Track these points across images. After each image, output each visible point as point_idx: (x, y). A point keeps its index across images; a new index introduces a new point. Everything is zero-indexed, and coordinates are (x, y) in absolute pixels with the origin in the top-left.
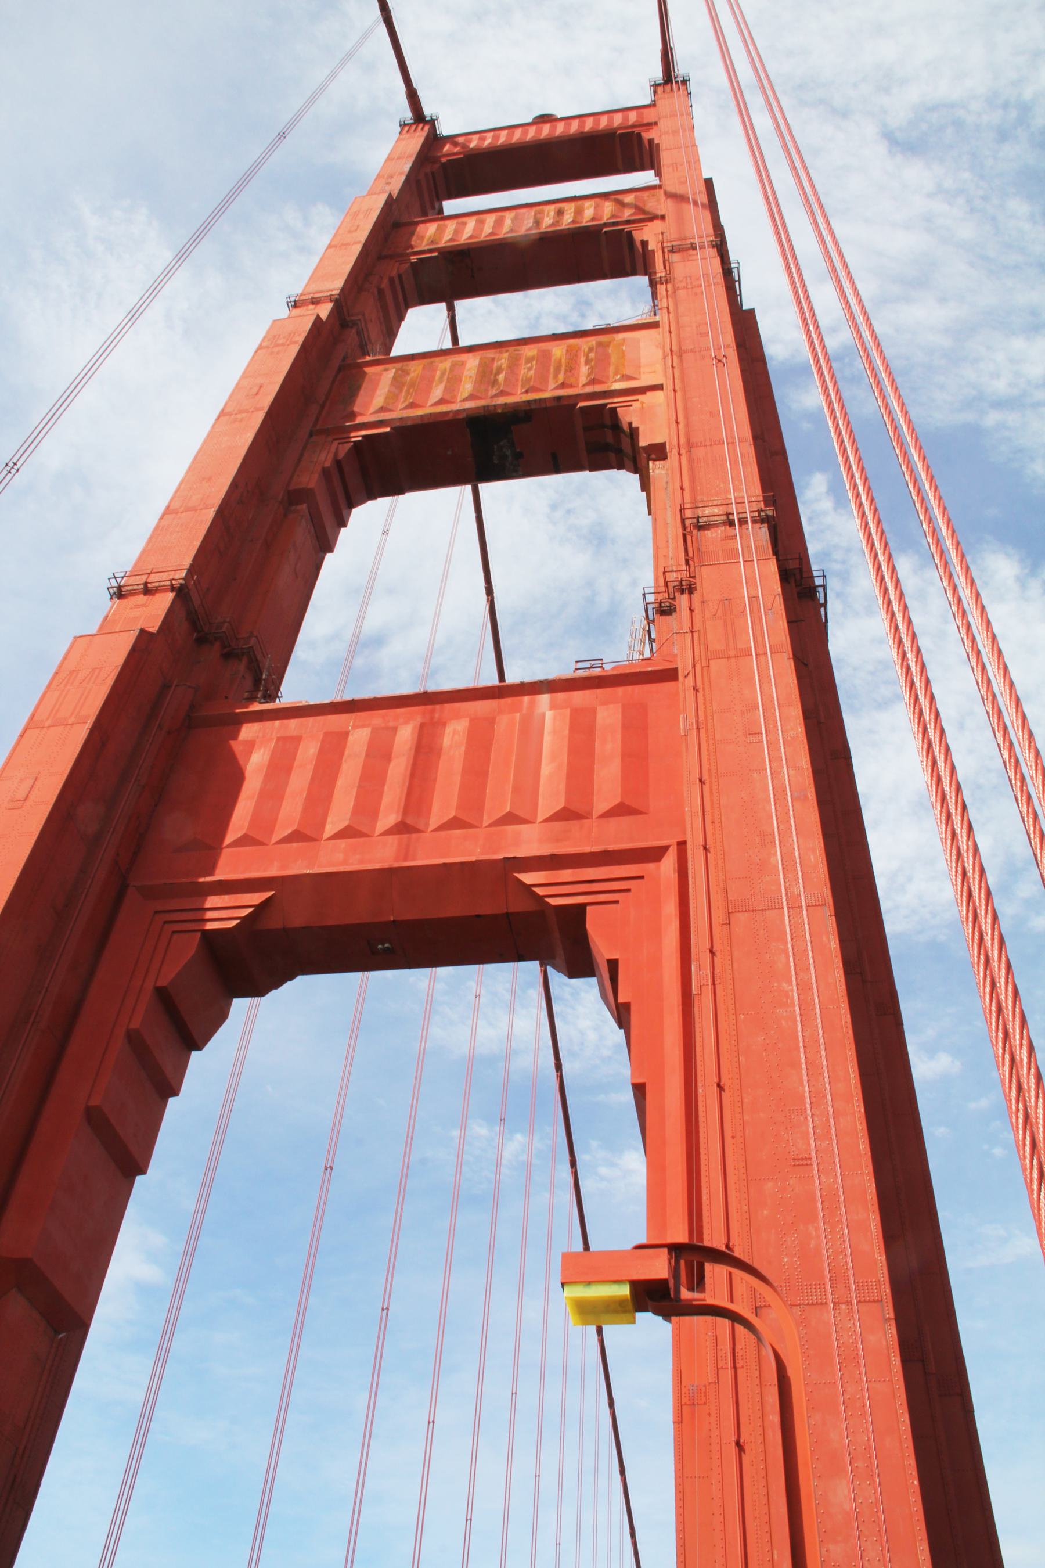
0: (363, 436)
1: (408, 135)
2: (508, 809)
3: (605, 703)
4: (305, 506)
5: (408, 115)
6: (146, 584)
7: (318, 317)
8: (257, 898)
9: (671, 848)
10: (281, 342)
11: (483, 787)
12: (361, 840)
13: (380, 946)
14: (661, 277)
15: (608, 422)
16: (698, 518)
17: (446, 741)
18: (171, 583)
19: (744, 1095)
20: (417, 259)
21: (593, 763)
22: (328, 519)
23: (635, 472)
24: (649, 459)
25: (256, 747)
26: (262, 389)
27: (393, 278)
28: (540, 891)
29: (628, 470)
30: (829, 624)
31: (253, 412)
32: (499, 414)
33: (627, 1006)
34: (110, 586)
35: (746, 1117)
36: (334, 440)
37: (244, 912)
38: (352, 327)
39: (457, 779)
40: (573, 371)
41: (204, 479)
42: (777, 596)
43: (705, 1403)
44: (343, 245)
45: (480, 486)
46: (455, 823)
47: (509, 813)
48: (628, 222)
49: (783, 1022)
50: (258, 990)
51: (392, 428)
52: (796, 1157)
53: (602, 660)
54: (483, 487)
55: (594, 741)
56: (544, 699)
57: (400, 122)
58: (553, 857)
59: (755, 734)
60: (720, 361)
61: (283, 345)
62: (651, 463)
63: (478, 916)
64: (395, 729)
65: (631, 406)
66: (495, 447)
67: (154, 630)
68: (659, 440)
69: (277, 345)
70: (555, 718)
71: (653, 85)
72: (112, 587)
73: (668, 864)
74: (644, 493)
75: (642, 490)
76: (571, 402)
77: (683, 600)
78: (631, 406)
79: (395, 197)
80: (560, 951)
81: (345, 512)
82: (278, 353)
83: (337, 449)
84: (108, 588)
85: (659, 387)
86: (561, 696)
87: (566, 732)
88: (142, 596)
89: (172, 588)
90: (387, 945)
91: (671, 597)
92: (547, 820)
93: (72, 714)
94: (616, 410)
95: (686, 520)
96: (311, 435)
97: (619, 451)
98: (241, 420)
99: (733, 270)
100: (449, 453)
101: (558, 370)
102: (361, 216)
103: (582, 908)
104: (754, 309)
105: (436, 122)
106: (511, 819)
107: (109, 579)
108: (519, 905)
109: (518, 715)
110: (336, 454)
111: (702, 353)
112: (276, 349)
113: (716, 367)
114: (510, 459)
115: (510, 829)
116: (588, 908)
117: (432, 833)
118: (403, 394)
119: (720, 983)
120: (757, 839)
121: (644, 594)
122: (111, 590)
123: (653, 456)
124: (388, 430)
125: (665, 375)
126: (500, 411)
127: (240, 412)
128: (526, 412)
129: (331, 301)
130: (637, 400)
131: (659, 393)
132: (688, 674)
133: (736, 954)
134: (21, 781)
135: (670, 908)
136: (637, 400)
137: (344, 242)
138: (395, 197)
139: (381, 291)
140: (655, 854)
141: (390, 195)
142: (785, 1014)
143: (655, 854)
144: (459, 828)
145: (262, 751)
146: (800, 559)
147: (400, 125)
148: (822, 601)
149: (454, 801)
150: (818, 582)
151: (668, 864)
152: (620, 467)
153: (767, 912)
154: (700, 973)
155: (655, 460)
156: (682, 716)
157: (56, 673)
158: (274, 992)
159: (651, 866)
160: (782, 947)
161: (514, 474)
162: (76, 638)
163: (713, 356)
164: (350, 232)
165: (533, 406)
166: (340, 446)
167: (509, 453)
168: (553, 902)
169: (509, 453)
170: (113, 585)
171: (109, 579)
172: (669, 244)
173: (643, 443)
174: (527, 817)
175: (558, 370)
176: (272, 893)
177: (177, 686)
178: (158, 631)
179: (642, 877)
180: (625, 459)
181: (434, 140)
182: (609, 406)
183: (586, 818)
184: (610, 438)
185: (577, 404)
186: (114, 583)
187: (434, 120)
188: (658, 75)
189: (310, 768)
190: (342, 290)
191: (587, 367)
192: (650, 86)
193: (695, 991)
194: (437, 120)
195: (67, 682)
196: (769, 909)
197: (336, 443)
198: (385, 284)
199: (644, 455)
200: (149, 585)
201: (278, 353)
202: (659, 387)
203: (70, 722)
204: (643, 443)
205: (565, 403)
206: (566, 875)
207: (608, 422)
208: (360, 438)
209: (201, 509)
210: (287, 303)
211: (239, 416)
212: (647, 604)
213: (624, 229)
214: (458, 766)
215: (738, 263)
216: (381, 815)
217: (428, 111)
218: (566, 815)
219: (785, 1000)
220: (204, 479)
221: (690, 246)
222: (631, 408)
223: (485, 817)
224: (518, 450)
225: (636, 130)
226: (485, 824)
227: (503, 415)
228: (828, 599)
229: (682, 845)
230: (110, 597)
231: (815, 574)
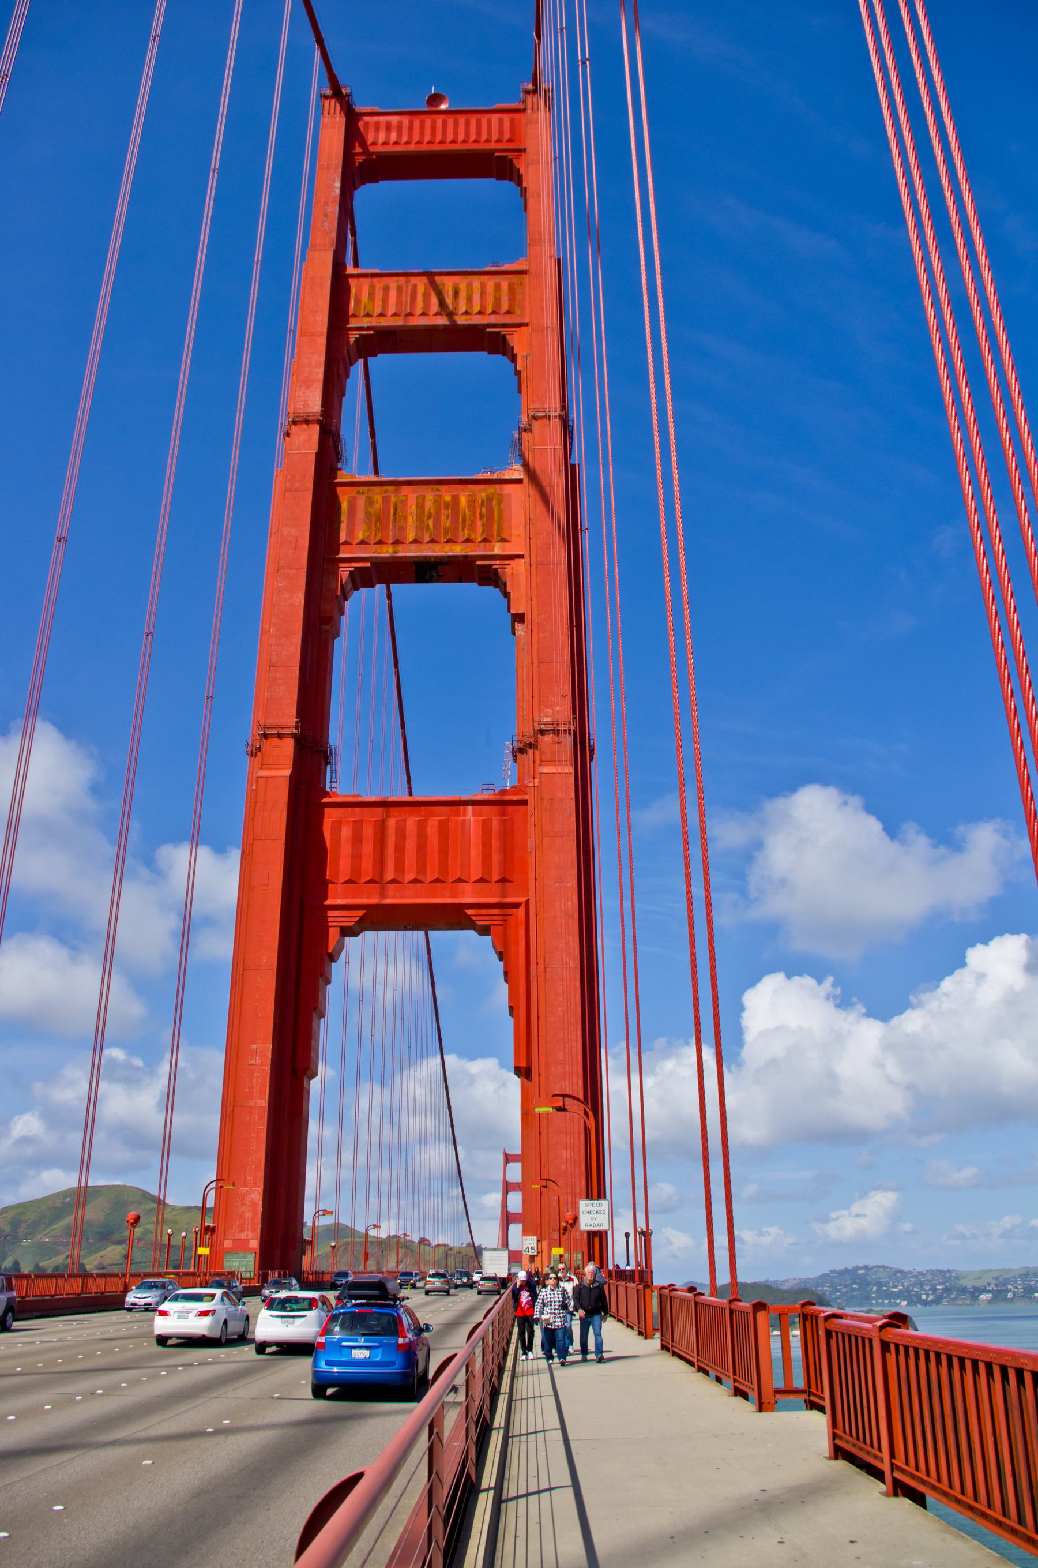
12: (400, 885)
20: (361, 335)
28: (473, 918)
29: (514, 183)
46: (437, 881)
68: (521, 611)
73: (521, 911)
85: (521, 557)
88: (276, 739)
106: (460, 880)
115: (460, 885)
123: (517, 620)
126: (433, 560)
135: (522, 932)
140: (517, 905)
151: (521, 911)
155: (518, 622)
159: (515, 910)
174: (467, 880)
185: (476, 561)
202: (521, 557)
206: (483, 911)
213: (500, 332)
214: (436, 847)
226: (450, 881)
229: (527, 901)
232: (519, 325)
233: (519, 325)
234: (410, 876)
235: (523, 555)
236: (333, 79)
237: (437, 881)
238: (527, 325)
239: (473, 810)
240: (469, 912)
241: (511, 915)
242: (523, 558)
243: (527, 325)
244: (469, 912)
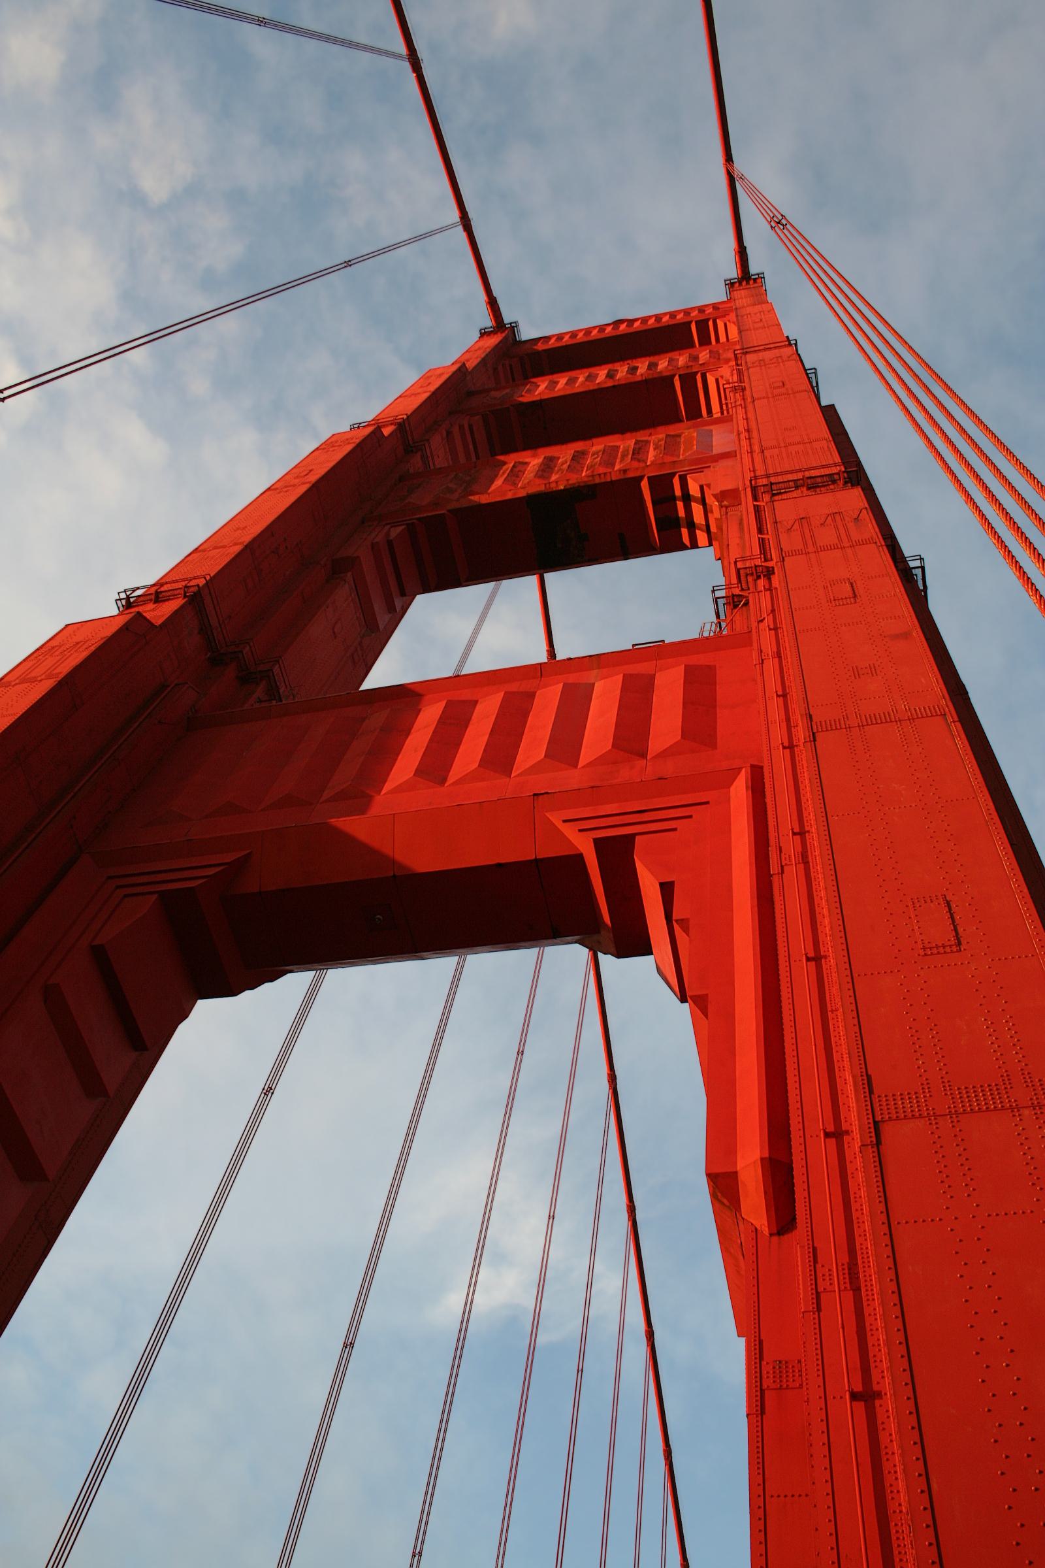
4: (349, 574)
6: (157, 593)
22: (378, 606)
26: (312, 473)
30: (929, 592)
32: (561, 490)
34: (118, 598)
36: (387, 524)
37: (211, 872)
42: (864, 511)
43: (801, 1386)
44: (413, 394)
45: (545, 575)
52: (927, 946)
54: (548, 577)
57: (480, 330)
61: (339, 446)
71: (728, 284)
72: (120, 599)
73: (740, 789)
83: (389, 530)
101: (624, 456)
102: (433, 378)
103: (630, 838)
105: (515, 328)
107: (119, 593)
110: (388, 534)
116: (637, 837)
121: (713, 591)
122: (119, 602)
127: (286, 487)
139: (449, 433)
146: (891, 535)
157: (38, 649)
158: (247, 994)
162: (67, 626)
164: (421, 387)
166: (393, 528)
170: (121, 598)
171: (119, 593)
175: (624, 456)
177: (176, 685)
179: (708, 803)
186: (123, 596)
187: (514, 327)
188: (733, 272)
192: (726, 285)
193: (774, 868)
194: (516, 327)
197: (388, 526)
199: (717, 503)
201: (334, 450)
211: (286, 489)
212: (716, 599)
217: (507, 318)
228: (928, 584)
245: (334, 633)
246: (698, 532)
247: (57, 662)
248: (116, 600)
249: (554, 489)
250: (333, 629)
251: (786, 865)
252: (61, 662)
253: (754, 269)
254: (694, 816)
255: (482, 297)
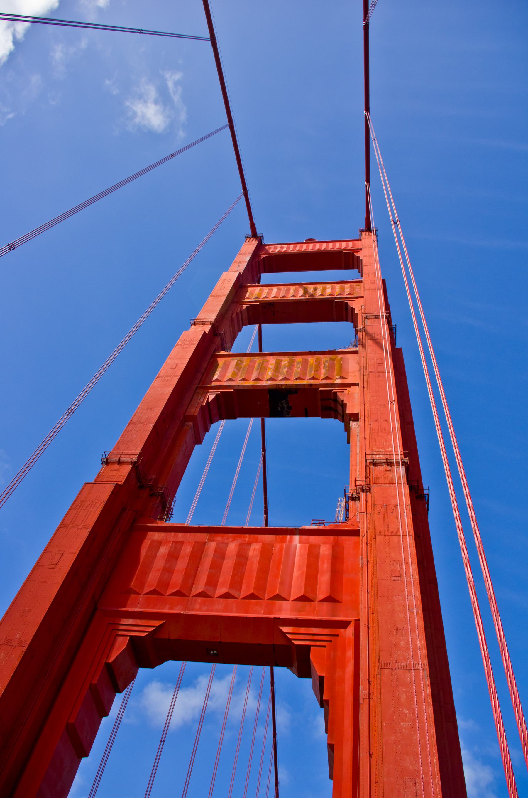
0: (221, 392)
1: (249, 243)
2: (277, 593)
3: (324, 543)
5: (249, 233)
6: (119, 459)
7: (205, 332)
8: (158, 623)
9: (352, 622)
10: (187, 343)
11: (266, 579)
12: (208, 599)
13: (212, 652)
14: (360, 329)
15: (332, 398)
16: (373, 460)
17: (251, 553)
18: (131, 460)
19: (384, 767)
21: (317, 573)
23: (343, 422)
24: (350, 420)
25: (162, 544)
27: (238, 313)
28: (289, 636)
31: (173, 377)
33: (327, 702)
34: (102, 458)
35: (385, 779)
38: (218, 336)
39: (255, 574)
40: (318, 371)
41: (149, 408)
44: (217, 296)
46: (252, 596)
47: (278, 594)
48: (346, 298)
49: (404, 730)
50: (151, 665)
51: (234, 390)
53: (324, 520)
55: (318, 562)
56: (297, 538)
57: (246, 236)
58: (297, 620)
59: (396, 576)
60: (392, 402)
61: (188, 344)
62: (351, 422)
63: (259, 644)
64: (227, 544)
65: (344, 392)
66: (280, 403)
67: (121, 483)
68: (356, 411)
69: (186, 345)
70: (301, 548)
74: (346, 432)
75: (345, 431)
76: (317, 387)
77: (363, 495)
78: (344, 392)
79: (241, 274)
80: (296, 664)
81: (209, 425)
82: (186, 348)
84: (101, 459)
86: (305, 537)
87: (306, 556)
89: (131, 463)
90: (215, 652)
91: (358, 492)
92: (294, 600)
93: (82, 523)
94: (337, 394)
95: (368, 460)
96: (197, 389)
97: (336, 411)
98: (167, 380)
99: (393, 328)
100: (259, 403)
102: (226, 282)
103: (308, 647)
104: (401, 348)
105: (262, 237)
106: (278, 597)
108: (280, 642)
109: (284, 544)
111: (379, 374)
112: (185, 346)
113: (390, 405)
114: (286, 409)
115: (278, 602)
116: (311, 648)
117: (242, 600)
118: (240, 373)
119: (372, 699)
120: (395, 631)
122: (103, 460)
123: (352, 419)
124: (232, 390)
125: (360, 379)
126: (283, 387)
127: (167, 376)
128: (295, 389)
129: (211, 324)
130: (347, 390)
131: (357, 388)
132: (364, 535)
133: (383, 690)
134: (55, 554)
135: (350, 653)
136: (347, 390)
137: (218, 295)
138: (241, 274)
140: (345, 625)
141: (240, 273)
142: (404, 726)
143: (345, 625)
144: (254, 599)
145: (165, 547)
146: (418, 481)
147: (246, 238)
148: (427, 501)
149: (253, 584)
150: (426, 492)
151: (350, 631)
152: (336, 418)
153: (398, 670)
154: (363, 692)
155: (353, 421)
156: (360, 556)
157: (75, 501)
159: (342, 630)
160: (404, 690)
161: (287, 416)
163: (389, 400)
164: (221, 289)
165: (299, 387)
167: (285, 406)
168: (296, 642)
169: (285, 406)
171: (102, 454)
172: (365, 315)
173: (348, 412)
176: (164, 622)
178: (123, 484)
180: (338, 415)
181: (260, 246)
182: (333, 391)
183: (313, 601)
184: (332, 404)
185: (319, 388)
187: (261, 237)
189: (187, 559)
190: (216, 319)
191: (324, 370)
195: (80, 506)
196: (399, 669)
198: (234, 316)
199: (348, 417)
200: (121, 460)
201: (186, 348)
203: (81, 527)
204: (348, 412)
205: (313, 387)
206: (302, 630)
207: (332, 398)
208: (219, 393)
209: (146, 424)
210: (191, 322)
211: (166, 378)
214: (255, 567)
215: (396, 325)
216: (218, 587)
217: (259, 232)
218: (303, 598)
219: (404, 718)
220: (149, 408)
221: (375, 316)
222: (343, 393)
223: (266, 595)
224: (290, 405)
225: (352, 252)
227: (285, 389)
229: (357, 621)
230: (101, 463)
231: (424, 488)
232: (357, 298)
233: (357, 298)
234: (222, 590)
235: (358, 384)
236: (253, 226)
237: (252, 596)
238: (362, 297)
239: (300, 538)
240: (285, 629)
241: (337, 635)
242: (358, 386)
243: (362, 297)
244: (285, 629)
245: (185, 454)
246: (338, 405)
247: (85, 517)
248: (101, 459)
249: (280, 388)
250: (185, 453)
251: (365, 698)
252: (87, 515)
253: (373, 226)
254: (333, 641)
255: (248, 222)
